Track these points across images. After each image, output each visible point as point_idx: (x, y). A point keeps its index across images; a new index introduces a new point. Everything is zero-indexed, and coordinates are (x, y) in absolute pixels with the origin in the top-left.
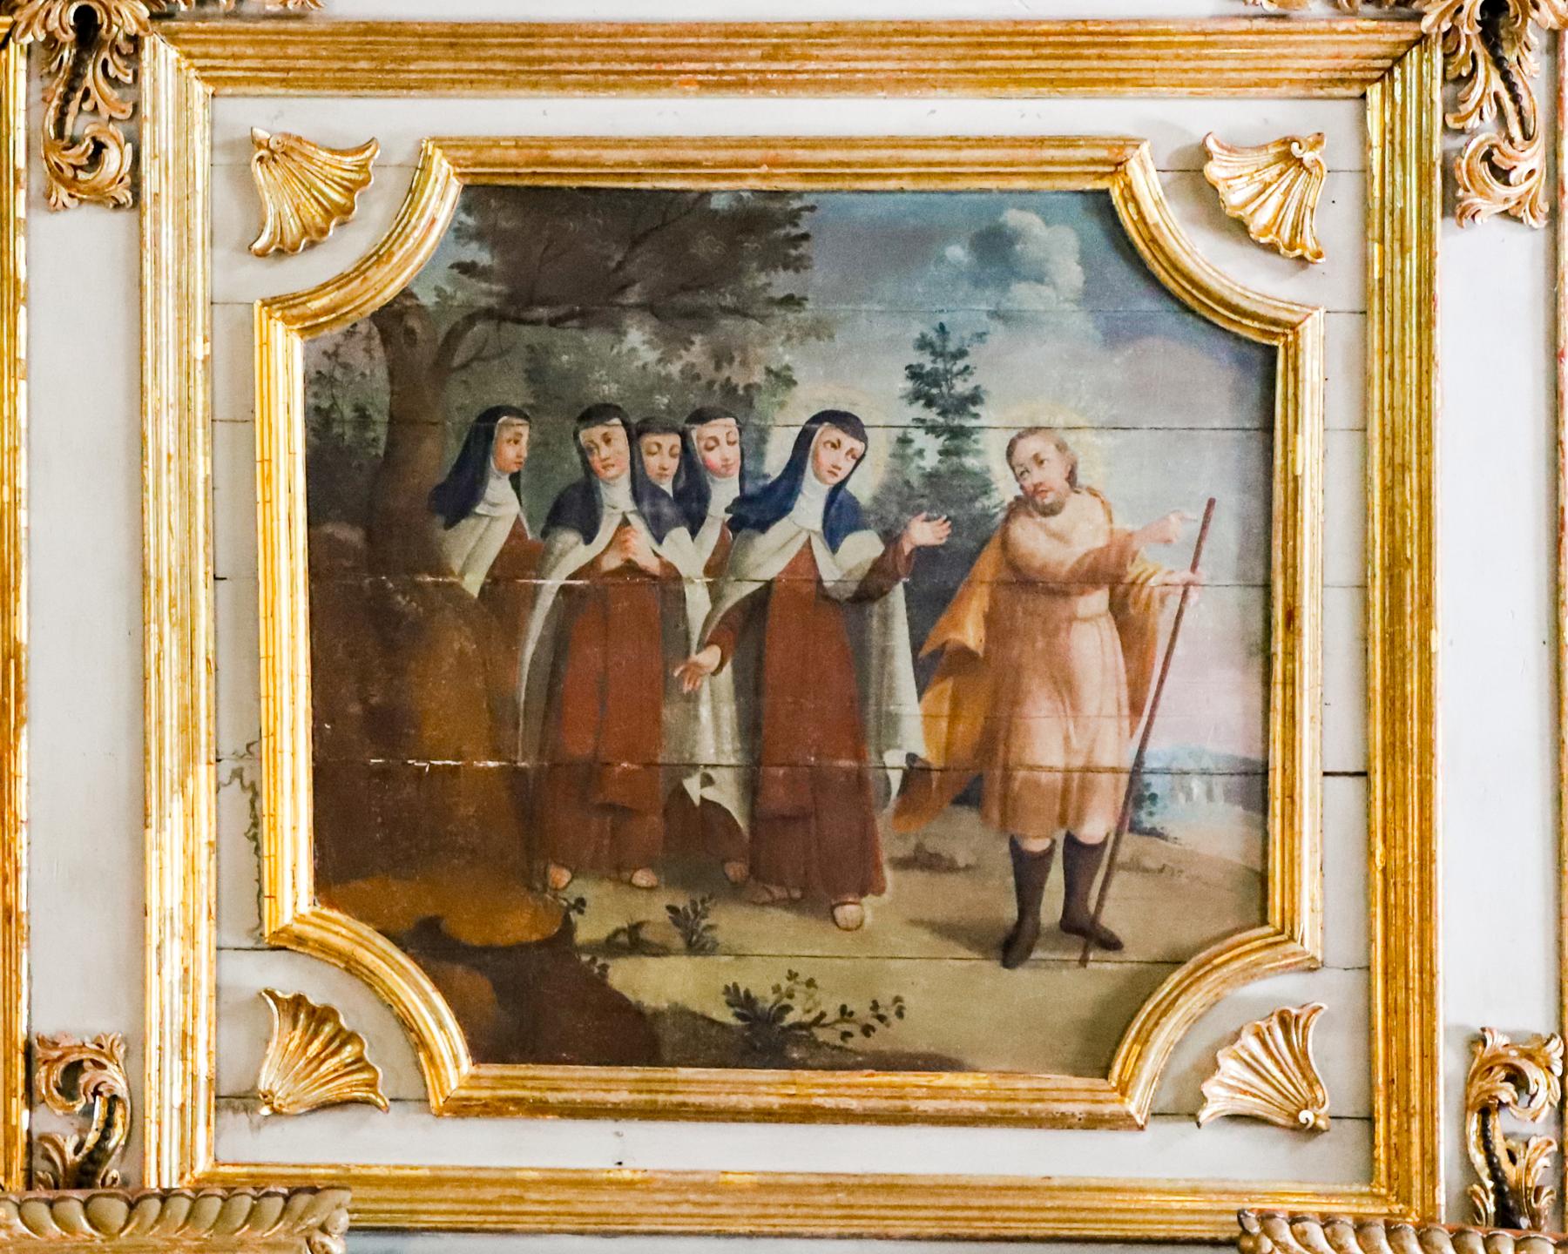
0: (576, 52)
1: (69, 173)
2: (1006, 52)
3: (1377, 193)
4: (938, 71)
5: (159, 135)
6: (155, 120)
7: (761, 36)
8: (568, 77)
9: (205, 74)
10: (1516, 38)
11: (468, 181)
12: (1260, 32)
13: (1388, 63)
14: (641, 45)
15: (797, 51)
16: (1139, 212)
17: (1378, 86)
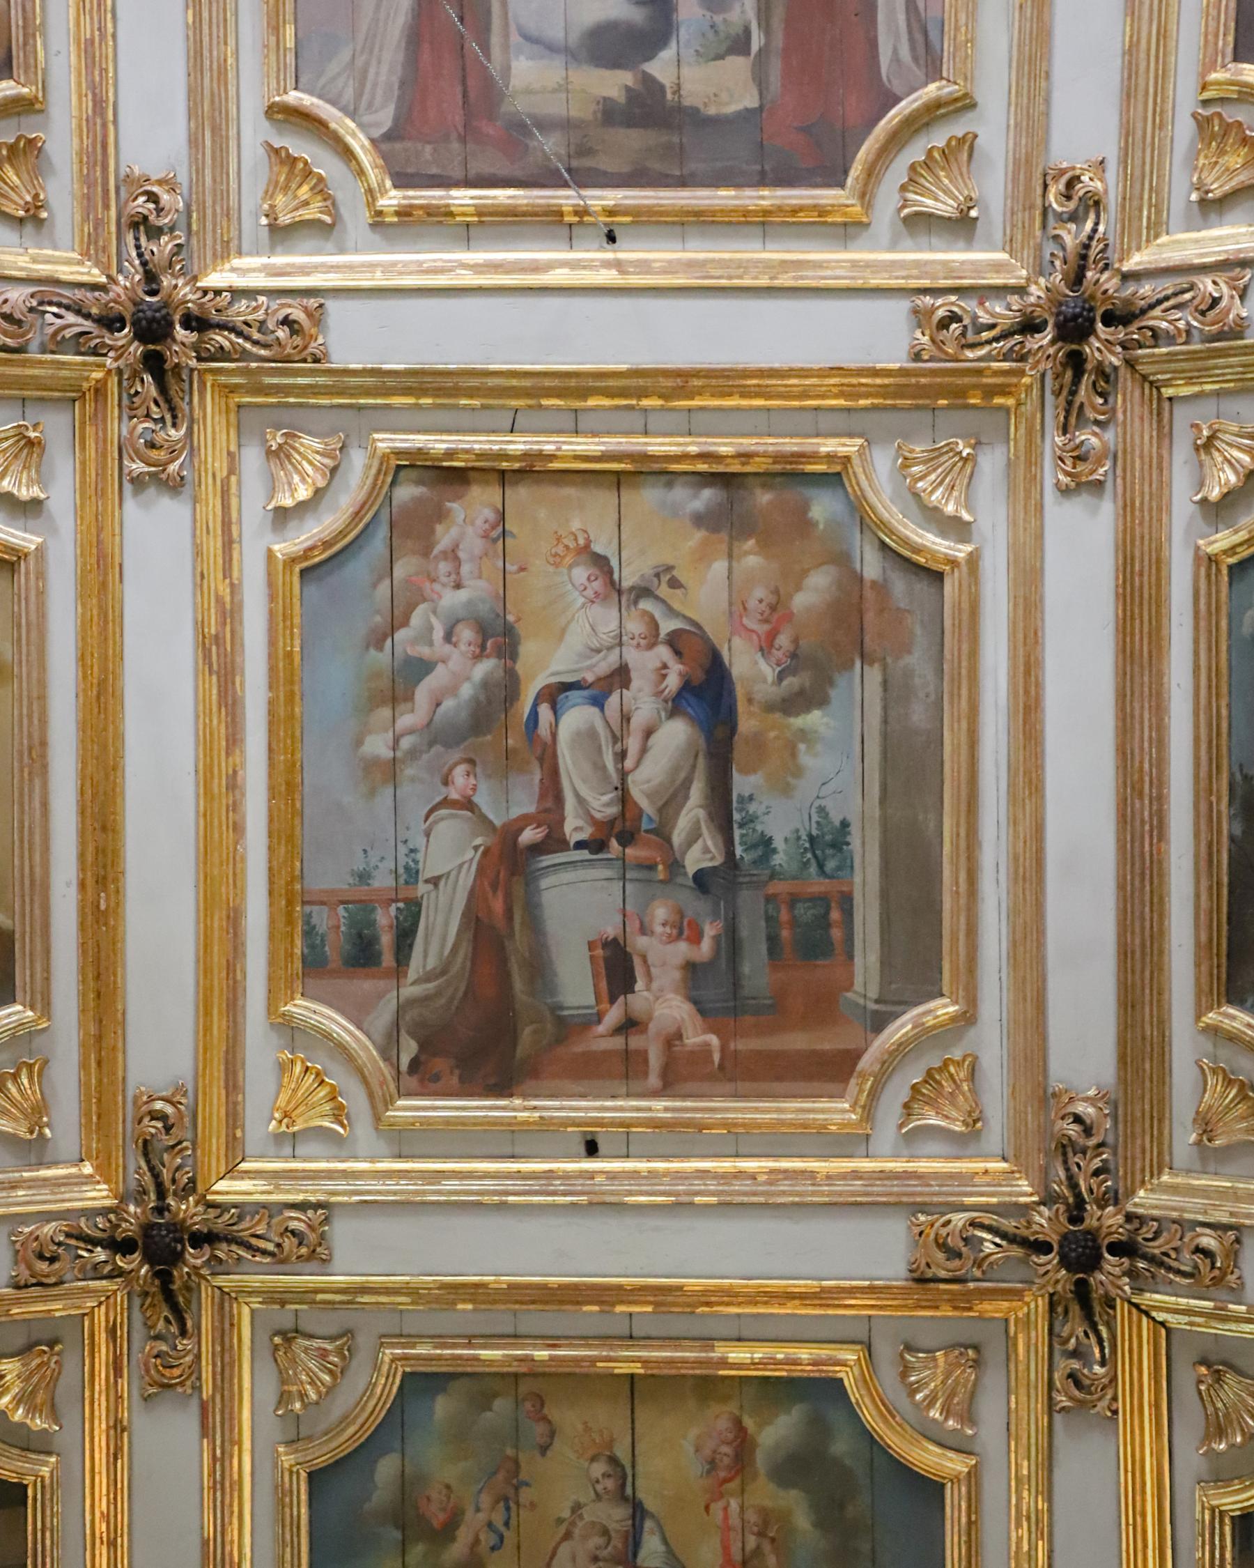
0: (1137, 924)
1: (1216, 1273)
2: (1137, 638)
3: (1232, 385)
4: (1151, 683)
5: (1193, 1208)
6: (1183, 1210)
7: (1126, 800)
8: (1155, 929)
9: (1155, 1172)
10: (1127, 302)
11: (1223, 1000)
12: (1124, 470)
13: (1147, 386)
14: (1133, 879)
15: (1136, 777)
16: (1241, 544)
17: (1163, 390)
